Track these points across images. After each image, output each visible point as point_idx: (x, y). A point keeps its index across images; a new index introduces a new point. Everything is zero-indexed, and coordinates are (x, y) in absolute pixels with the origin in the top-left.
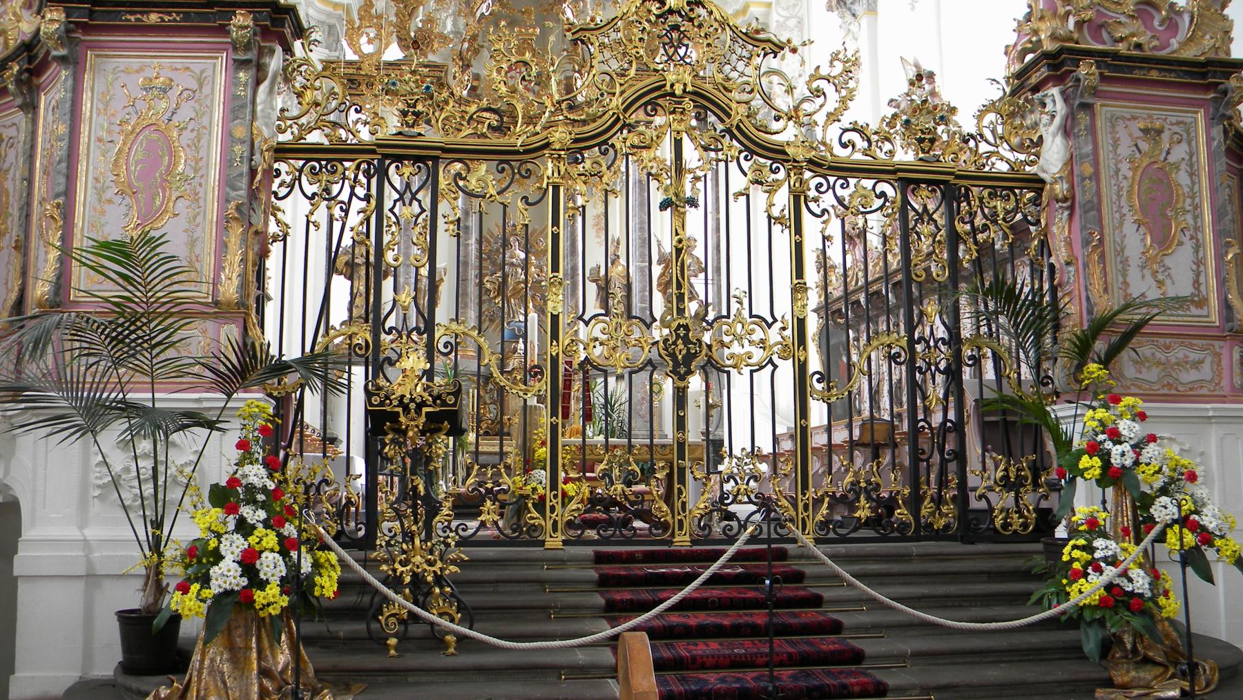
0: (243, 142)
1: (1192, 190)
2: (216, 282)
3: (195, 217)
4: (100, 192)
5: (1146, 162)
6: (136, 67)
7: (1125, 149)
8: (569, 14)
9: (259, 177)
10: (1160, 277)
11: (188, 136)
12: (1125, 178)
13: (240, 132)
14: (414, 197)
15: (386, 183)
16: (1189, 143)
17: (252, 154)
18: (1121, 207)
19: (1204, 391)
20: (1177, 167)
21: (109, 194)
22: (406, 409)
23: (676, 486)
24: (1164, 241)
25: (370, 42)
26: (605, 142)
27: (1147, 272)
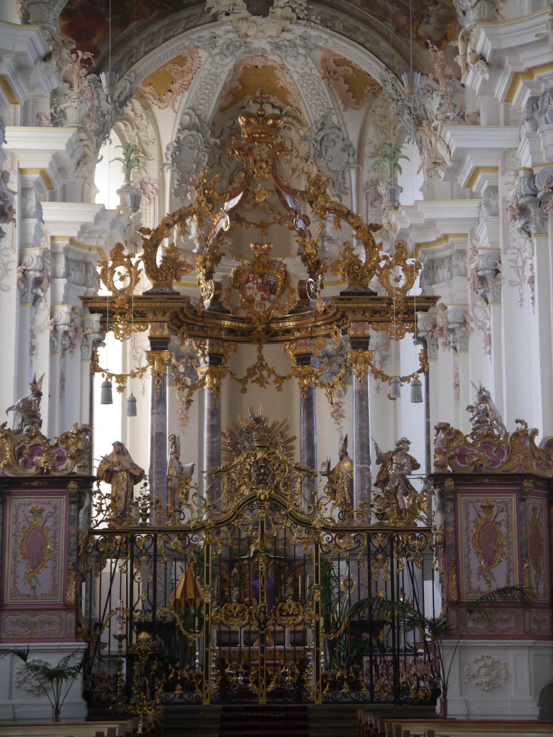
0: (74, 535)
1: (508, 535)
2: (65, 595)
3: (55, 568)
4: (15, 558)
5: (483, 523)
6: (27, 503)
7: (472, 518)
9: (81, 551)
10: (488, 578)
11: (50, 534)
12: (472, 531)
13: (73, 531)
14: (146, 551)
15: (135, 547)
16: (507, 512)
17: (78, 540)
18: (468, 546)
19: (511, 633)
20: (500, 524)
21: (18, 559)
22: (141, 652)
23: (260, 678)
24: (490, 562)
25: (122, 278)
26: (230, 523)
27: (481, 577)
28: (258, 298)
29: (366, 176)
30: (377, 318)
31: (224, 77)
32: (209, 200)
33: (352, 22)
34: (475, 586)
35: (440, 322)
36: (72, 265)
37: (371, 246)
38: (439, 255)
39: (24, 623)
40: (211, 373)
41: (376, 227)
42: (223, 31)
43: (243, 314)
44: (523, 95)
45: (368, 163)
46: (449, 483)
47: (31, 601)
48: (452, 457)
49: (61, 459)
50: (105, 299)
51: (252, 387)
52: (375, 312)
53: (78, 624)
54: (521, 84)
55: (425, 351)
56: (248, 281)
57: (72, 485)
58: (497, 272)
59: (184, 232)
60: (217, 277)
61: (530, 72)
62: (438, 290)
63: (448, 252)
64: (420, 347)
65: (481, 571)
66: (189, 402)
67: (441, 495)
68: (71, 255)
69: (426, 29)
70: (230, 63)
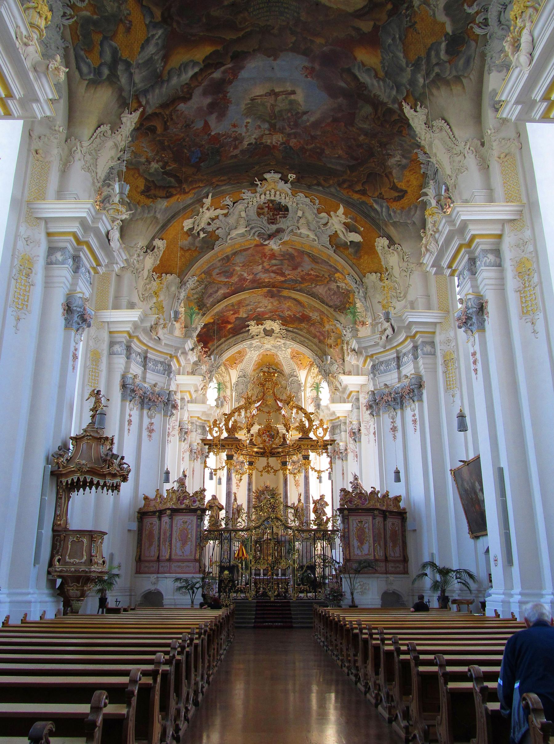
2: (195, 556)
7: (355, 526)
8: (283, 412)
13: (199, 530)
25: (217, 432)
28: (267, 440)
29: (308, 395)
30: (312, 448)
31: (255, 358)
32: (250, 403)
33: (302, 339)
34: (356, 553)
35: (336, 449)
36: (198, 427)
37: (310, 421)
38: (336, 424)
39: (179, 567)
40: (249, 469)
41: (312, 414)
42: (255, 342)
43: (261, 446)
44: (369, 364)
45: (308, 390)
46: (346, 512)
47: (181, 557)
48: (347, 502)
49: (194, 502)
50: (210, 440)
51: (264, 474)
52: (312, 446)
53: (201, 567)
54: (369, 360)
55: (331, 461)
56: (264, 434)
57: (199, 512)
58: (360, 430)
59: (239, 415)
60: (252, 432)
61: (372, 356)
62: (336, 437)
63: (339, 423)
64: (329, 459)
65: (358, 547)
66: (241, 479)
67: (343, 517)
68: (197, 423)
69: (330, 341)
70: (257, 353)
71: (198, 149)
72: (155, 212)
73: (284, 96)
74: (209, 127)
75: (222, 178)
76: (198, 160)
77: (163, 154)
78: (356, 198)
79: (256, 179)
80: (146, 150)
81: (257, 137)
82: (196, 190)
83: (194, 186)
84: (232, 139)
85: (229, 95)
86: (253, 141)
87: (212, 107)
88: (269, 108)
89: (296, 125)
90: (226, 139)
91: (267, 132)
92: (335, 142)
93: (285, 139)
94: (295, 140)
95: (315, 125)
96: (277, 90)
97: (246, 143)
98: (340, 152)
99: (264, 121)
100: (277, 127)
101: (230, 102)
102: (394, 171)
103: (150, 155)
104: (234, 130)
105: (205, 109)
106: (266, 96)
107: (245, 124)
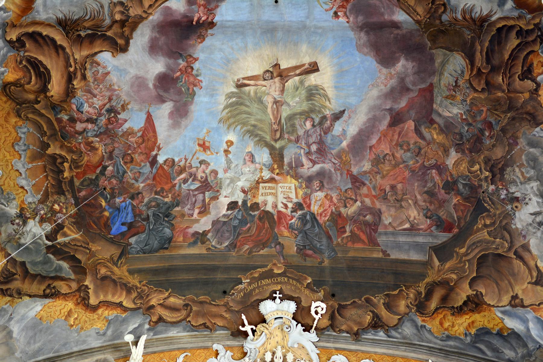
71: (128, 201)
72: (10, 319)
73: (297, 78)
74: (154, 131)
75: (172, 300)
76: (124, 229)
77: (55, 202)
78: (462, 329)
79: (244, 317)
80: (23, 183)
81: (247, 185)
82: (111, 314)
83: (110, 298)
84: (197, 185)
85: (196, 66)
86: (239, 197)
87: (165, 81)
88: (269, 110)
89: (322, 151)
90: (185, 181)
91: (267, 175)
92: (399, 186)
93: (301, 193)
94: (320, 195)
95: (359, 143)
96: (284, 65)
97: (224, 200)
98: (413, 213)
99: (262, 142)
100: (286, 160)
101: (196, 83)
102: (533, 242)
103: (30, 200)
104: (202, 156)
105: (151, 86)
106: (265, 80)
107: (225, 146)
